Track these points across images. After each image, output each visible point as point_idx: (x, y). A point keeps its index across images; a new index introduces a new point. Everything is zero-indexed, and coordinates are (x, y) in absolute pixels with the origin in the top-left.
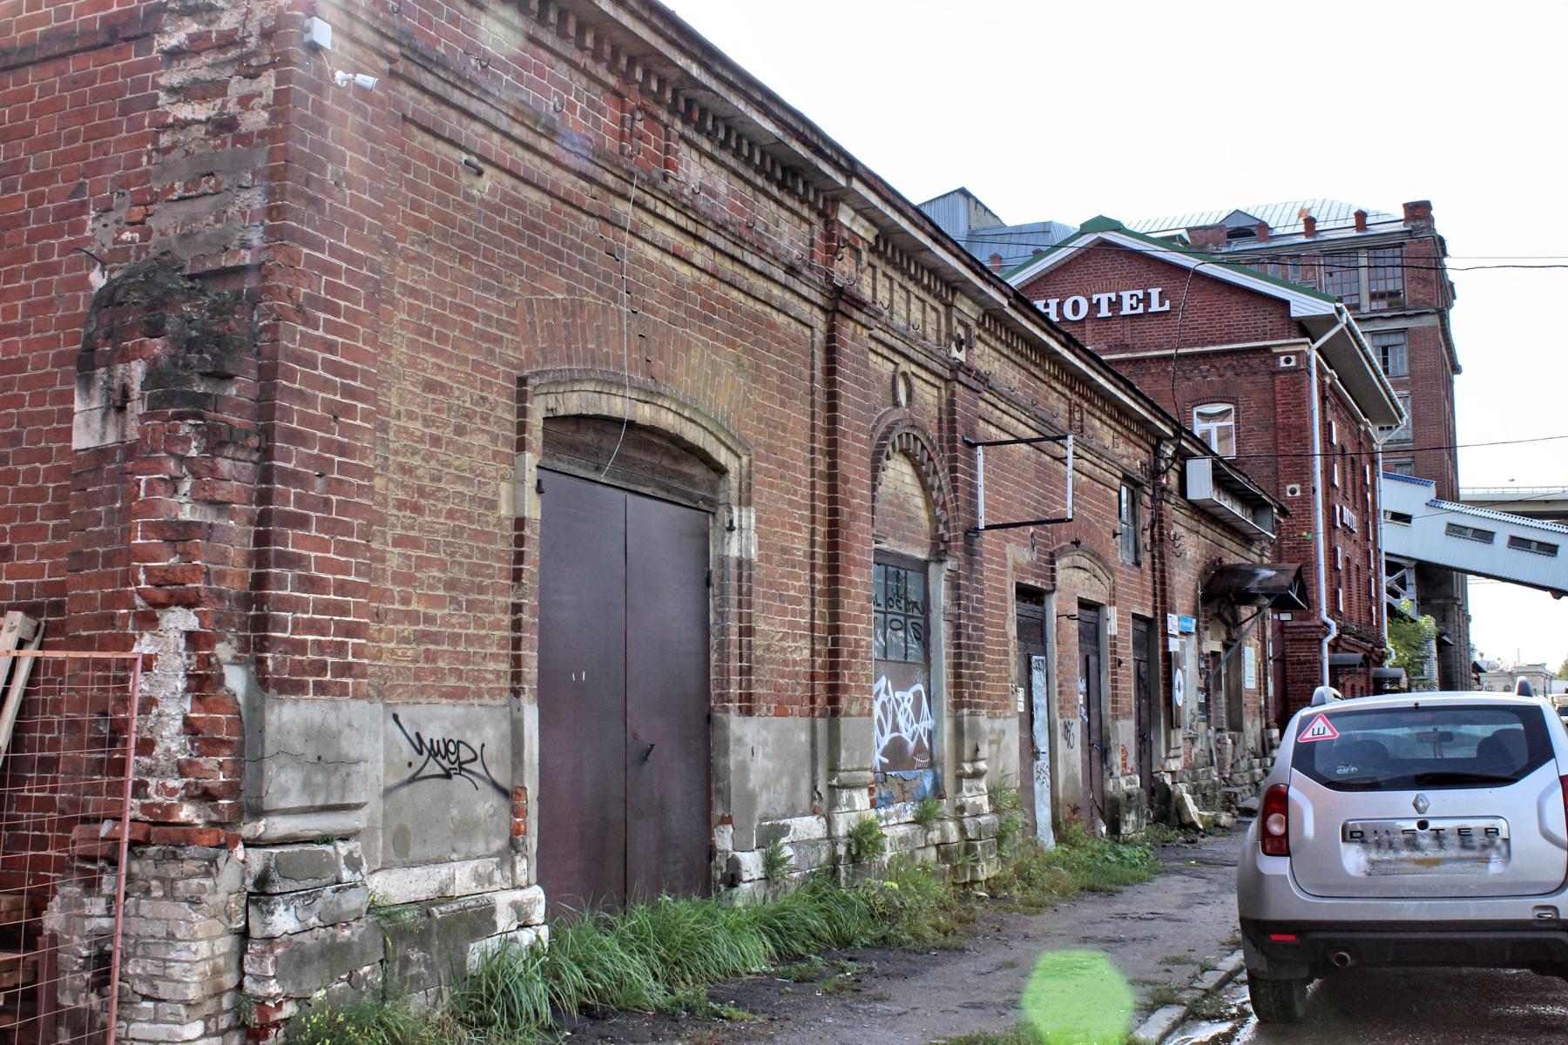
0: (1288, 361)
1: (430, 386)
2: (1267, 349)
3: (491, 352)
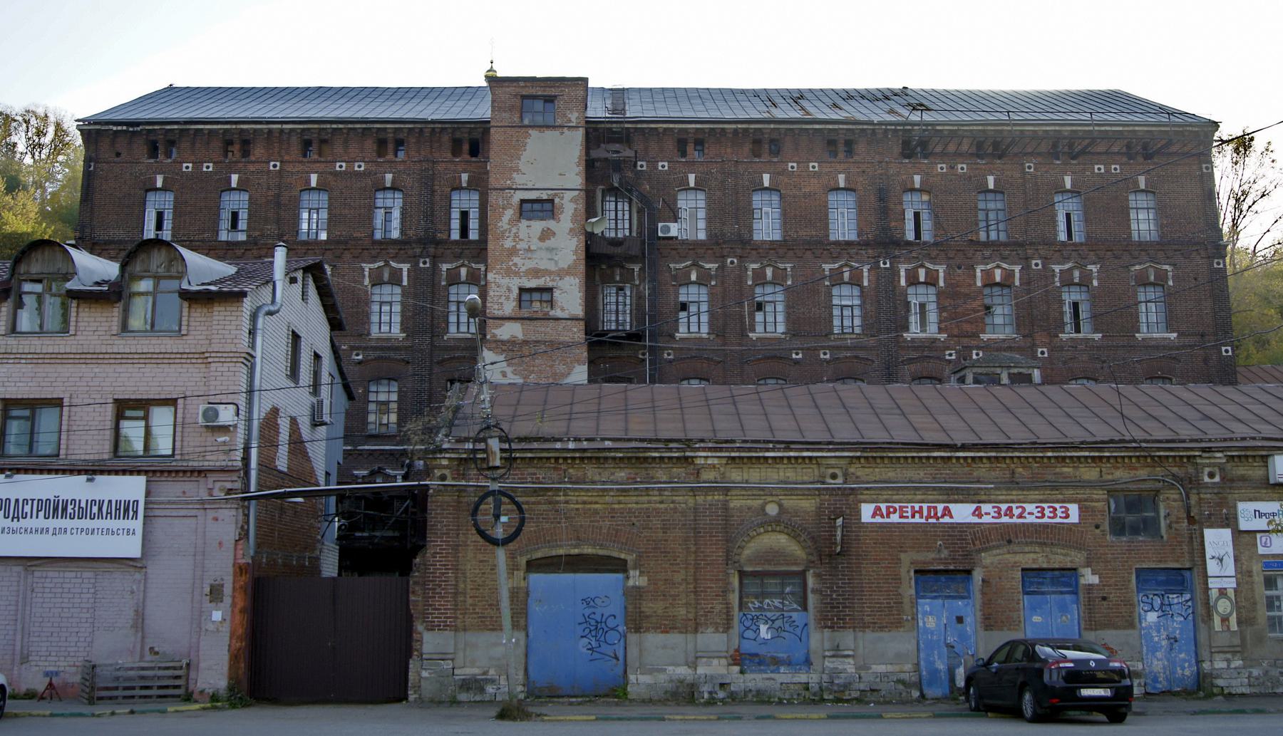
1: (481, 561)
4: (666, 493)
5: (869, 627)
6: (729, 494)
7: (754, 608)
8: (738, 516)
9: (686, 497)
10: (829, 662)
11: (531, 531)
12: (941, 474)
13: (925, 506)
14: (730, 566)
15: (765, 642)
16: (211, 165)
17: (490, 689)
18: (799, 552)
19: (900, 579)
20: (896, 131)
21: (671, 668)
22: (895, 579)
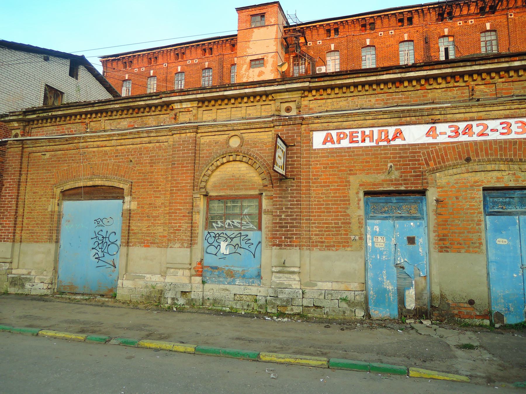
1: (34, 193)
3: (48, 184)
4: (152, 134)
5: (317, 246)
6: (199, 131)
7: (217, 227)
8: (207, 150)
9: (168, 137)
10: (276, 277)
11: (64, 170)
12: (393, 99)
13: (376, 130)
14: (195, 191)
15: (224, 257)
16: (144, 68)
17: (28, 286)
18: (256, 178)
19: (349, 200)
20: (434, 8)
21: (148, 276)
22: (344, 201)
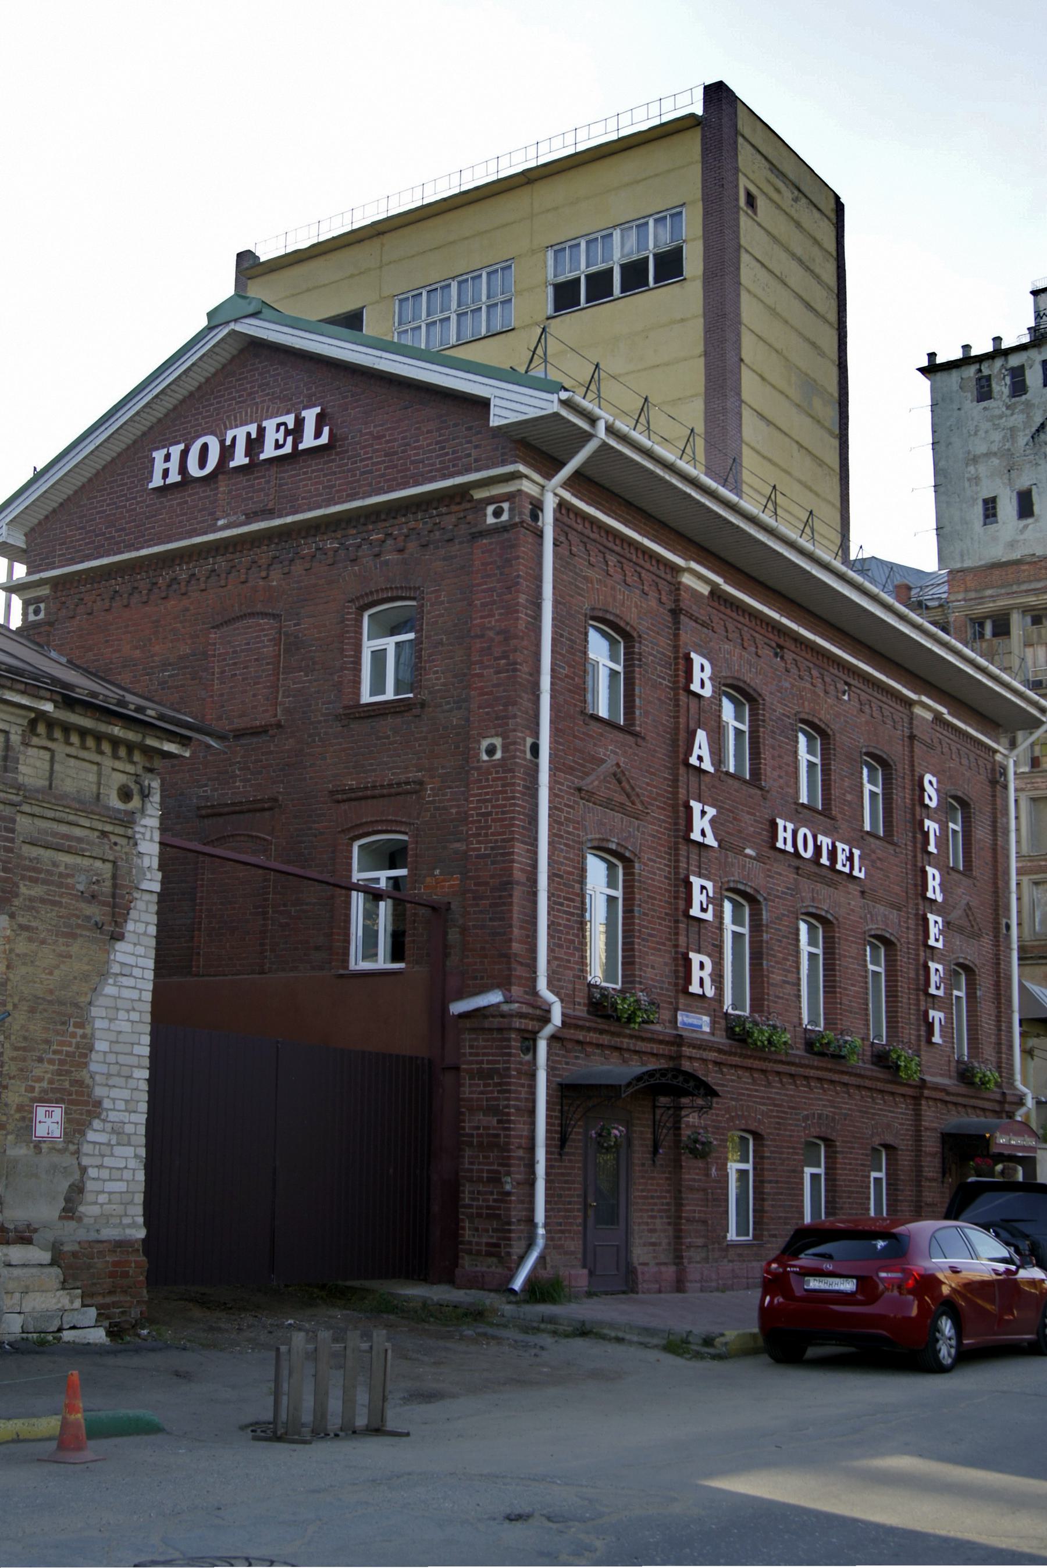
0: (497, 513)
2: (462, 493)
